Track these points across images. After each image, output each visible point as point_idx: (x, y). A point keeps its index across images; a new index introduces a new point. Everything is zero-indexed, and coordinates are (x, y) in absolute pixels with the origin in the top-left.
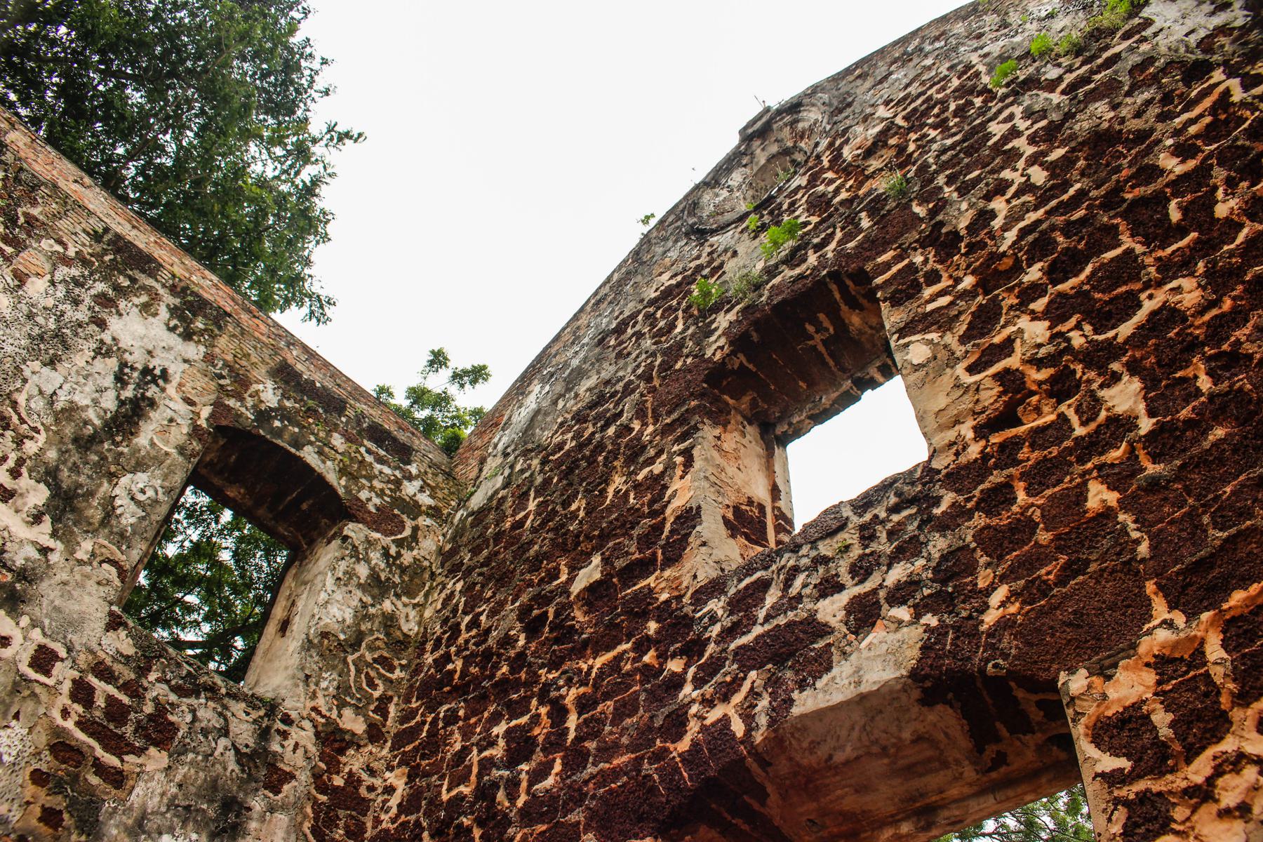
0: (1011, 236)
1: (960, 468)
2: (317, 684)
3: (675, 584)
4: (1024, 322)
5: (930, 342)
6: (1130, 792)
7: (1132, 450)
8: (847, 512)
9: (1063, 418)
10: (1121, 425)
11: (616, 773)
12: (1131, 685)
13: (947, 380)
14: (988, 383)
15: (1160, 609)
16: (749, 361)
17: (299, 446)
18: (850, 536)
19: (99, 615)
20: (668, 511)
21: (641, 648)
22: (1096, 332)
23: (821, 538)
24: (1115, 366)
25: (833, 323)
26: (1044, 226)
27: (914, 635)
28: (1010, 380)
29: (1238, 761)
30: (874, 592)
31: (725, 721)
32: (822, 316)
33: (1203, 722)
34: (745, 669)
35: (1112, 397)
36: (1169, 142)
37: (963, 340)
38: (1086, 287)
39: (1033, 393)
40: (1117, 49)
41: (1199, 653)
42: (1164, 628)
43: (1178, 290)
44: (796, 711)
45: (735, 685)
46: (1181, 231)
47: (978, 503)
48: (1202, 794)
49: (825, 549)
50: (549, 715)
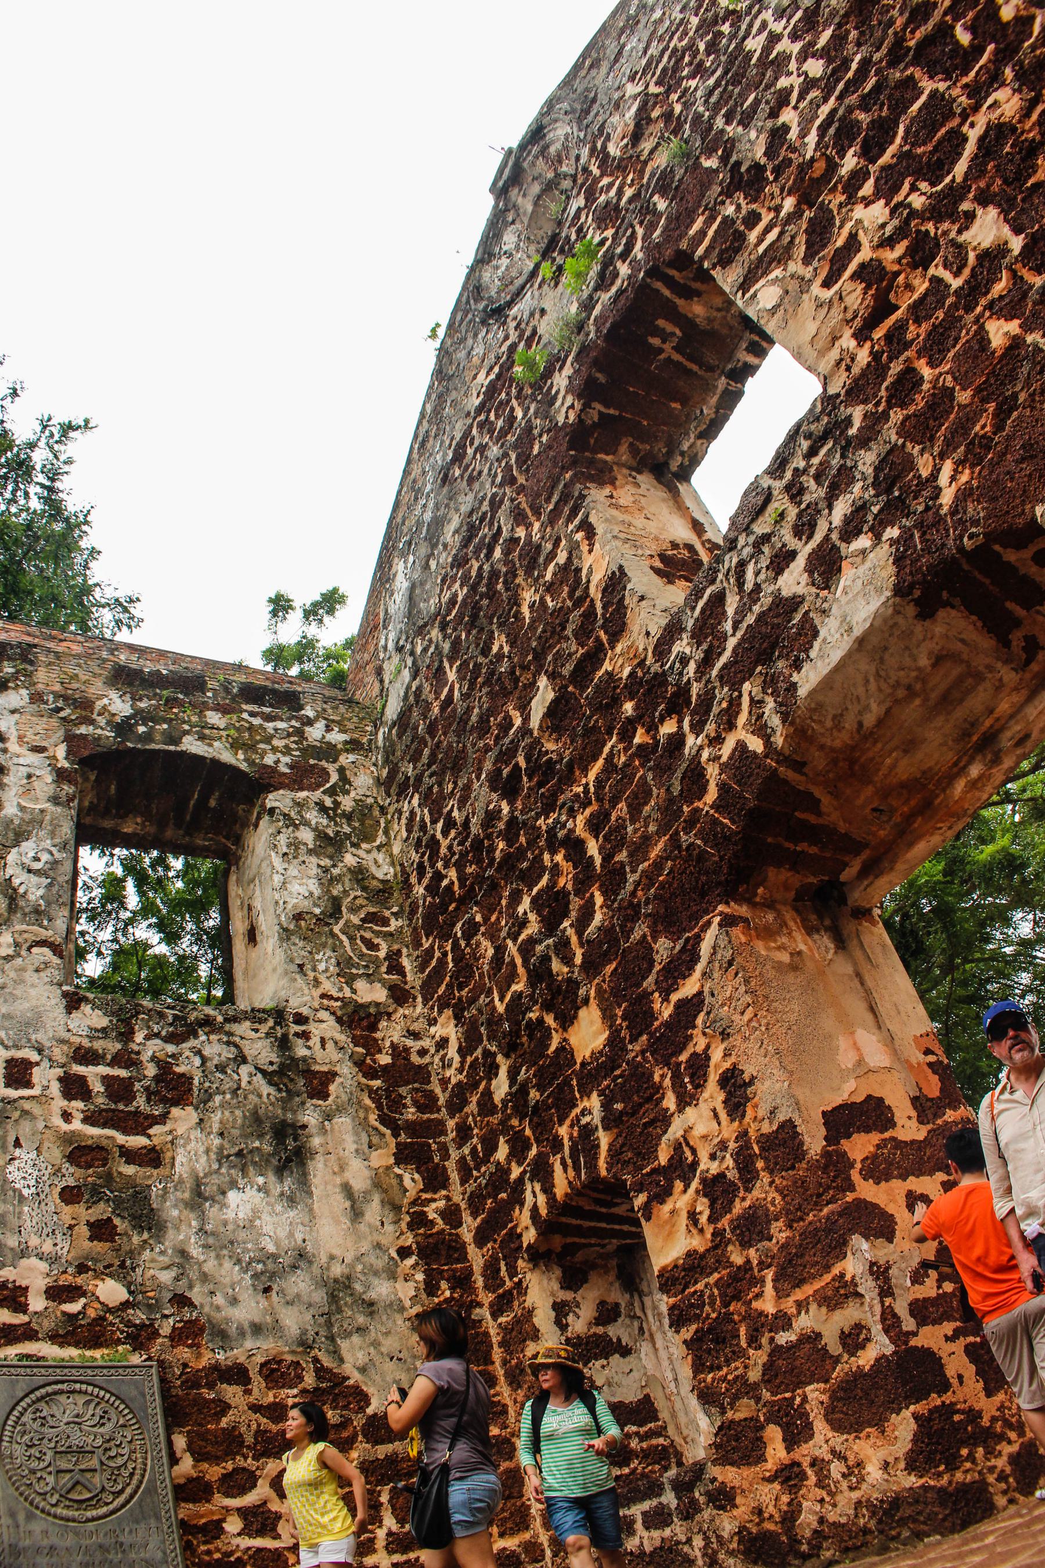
0: (812, 138)
1: (856, 380)
2: (314, 969)
4: (859, 212)
7: (1014, 274)
8: (766, 482)
9: (936, 281)
11: (658, 865)
13: (807, 304)
14: (849, 286)
16: (607, 407)
17: (177, 741)
19: (53, 1002)
21: (626, 736)
22: (933, 184)
23: (753, 520)
24: (965, 206)
25: (676, 324)
26: (840, 112)
27: (883, 554)
28: (871, 275)
30: (827, 538)
31: (741, 746)
32: (661, 323)
34: (736, 686)
35: (974, 237)
38: (907, 148)
39: (897, 274)
44: (802, 692)
45: (734, 705)
47: (888, 402)
50: (567, 858)
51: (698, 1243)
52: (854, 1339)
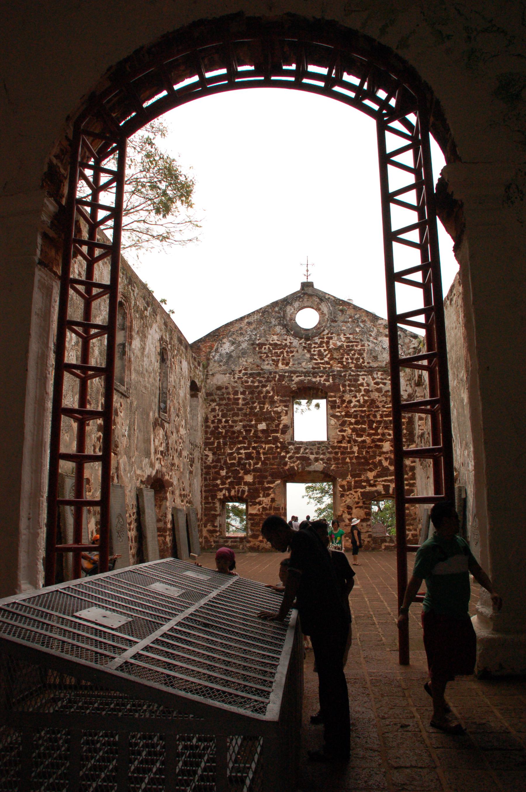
0: (353, 410)
3: (284, 439)
9: (347, 447)
10: (353, 452)
11: (274, 469)
12: (345, 483)
15: (349, 477)
18: (316, 447)
20: (282, 422)
26: (358, 413)
29: (352, 494)
31: (293, 466)
33: (349, 489)
34: (298, 460)
36: (381, 413)
37: (340, 425)
41: (351, 483)
42: (349, 478)
45: (296, 462)
46: (373, 429)
48: (348, 495)
49: (311, 447)
51: (258, 512)
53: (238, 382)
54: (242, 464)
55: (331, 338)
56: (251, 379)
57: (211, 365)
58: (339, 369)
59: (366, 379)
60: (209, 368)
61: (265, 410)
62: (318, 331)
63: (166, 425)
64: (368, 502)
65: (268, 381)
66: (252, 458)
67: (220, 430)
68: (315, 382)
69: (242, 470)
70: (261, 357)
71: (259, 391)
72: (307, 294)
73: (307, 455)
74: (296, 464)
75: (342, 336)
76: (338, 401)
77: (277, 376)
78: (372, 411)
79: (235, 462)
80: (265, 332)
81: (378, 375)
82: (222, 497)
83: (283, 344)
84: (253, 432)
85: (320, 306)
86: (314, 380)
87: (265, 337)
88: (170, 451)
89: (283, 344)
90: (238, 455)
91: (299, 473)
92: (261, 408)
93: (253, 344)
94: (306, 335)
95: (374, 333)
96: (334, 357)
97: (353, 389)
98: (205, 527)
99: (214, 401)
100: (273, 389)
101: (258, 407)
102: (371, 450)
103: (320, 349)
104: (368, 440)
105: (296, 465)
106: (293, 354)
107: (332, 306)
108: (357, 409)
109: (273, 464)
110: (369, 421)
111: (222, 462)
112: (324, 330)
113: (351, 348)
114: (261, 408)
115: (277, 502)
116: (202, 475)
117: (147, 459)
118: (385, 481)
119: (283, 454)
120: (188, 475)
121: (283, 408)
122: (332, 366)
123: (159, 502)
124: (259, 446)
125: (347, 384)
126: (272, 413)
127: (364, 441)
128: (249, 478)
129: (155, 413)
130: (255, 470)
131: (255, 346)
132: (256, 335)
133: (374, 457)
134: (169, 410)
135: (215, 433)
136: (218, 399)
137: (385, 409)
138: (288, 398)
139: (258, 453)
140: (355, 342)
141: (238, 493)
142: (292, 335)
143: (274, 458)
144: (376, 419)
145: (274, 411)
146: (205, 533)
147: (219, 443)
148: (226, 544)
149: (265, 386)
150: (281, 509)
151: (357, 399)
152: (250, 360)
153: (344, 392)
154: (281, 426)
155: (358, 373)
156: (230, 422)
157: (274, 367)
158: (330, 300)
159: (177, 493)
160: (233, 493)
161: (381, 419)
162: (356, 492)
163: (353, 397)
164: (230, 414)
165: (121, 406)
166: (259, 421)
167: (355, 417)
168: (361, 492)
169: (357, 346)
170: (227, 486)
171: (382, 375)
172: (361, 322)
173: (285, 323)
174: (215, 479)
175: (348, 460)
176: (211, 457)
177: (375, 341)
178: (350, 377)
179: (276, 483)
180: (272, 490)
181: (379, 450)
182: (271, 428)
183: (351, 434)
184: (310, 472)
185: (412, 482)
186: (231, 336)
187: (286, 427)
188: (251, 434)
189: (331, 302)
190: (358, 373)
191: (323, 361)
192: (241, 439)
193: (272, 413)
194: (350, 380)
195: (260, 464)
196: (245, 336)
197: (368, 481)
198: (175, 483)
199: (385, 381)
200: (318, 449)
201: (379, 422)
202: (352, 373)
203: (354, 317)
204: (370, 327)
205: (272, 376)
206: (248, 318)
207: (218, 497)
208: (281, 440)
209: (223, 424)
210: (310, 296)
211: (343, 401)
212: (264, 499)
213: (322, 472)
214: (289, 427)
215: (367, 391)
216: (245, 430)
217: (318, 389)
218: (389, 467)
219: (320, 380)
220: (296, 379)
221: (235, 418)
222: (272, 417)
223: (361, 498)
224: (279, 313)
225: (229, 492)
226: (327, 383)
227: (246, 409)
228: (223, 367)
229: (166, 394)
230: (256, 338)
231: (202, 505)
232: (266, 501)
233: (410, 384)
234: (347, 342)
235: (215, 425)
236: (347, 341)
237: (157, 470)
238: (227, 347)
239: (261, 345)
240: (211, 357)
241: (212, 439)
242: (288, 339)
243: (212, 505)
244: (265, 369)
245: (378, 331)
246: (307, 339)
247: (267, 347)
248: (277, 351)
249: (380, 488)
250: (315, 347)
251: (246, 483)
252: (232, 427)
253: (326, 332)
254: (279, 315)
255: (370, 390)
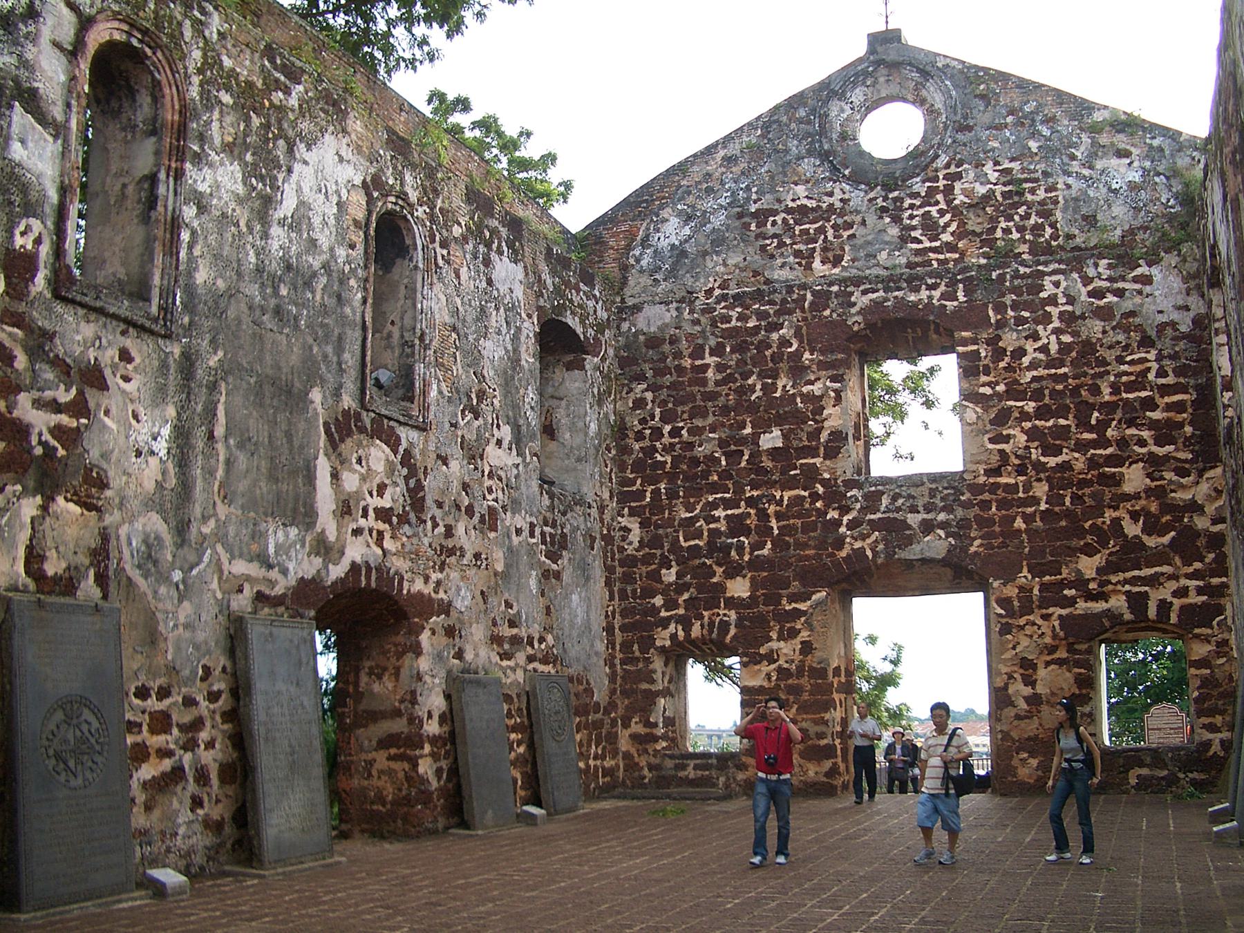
0: (1029, 375)
3: (832, 471)
5: (976, 413)
6: (1004, 621)
8: (925, 480)
10: (1035, 501)
11: (808, 558)
12: (1011, 591)
15: (1025, 572)
20: (826, 424)
24: (1042, 475)
26: (1044, 383)
29: (1034, 624)
33: (1027, 609)
36: (1112, 378)
37: (991, 422)
40: (1127, 285)
43: (1077, 459)
45: (869, 536)
46: (1091, 429)
48: (1022, 628)
49: (912, 491)
51: (766, 684)
52: (821, 736)
53: (703, 320)
54: (720, 550)
55: (959, 176)
56: (739, 310)
57: (631, 282)
58: (983, 261)
59: (1064, 284)
60: (627, 292)
61: (777, 395)
62: (918, 160)
63: (407, 435)
64: (1084, 647)
65: (784, 311)
66: (747, 532)
67: (659, 458)
68: (915, 305)
69: (720, 565)
70: (763, 248)
71: (761, 342)
72: (889, 64)
73: (898, 516)
74: (869, 541)
75: (988, 168)
76: (983, 354)
77: (809, 296)
78: (1085, 374)
79: (701, 544)
80: (772, 178)
81: (1100, 270)
82: (668, 643)
83: (824, 205)
84: (746, 457)
85: (924, 93)
86: (912, 298)
87: (773, 190)
88: (432, 510)
89: (824, 205)
90: (708, 524)
91: (878, 567)
92: (768, 389)
93: (740, 216)
94: (887, 178)
95: (1082, 148)
96: (970, 227)
97: (1026, 314)
98: (626, 725)
99: (641, 377)
100: (798, 334)
101: (758, 387)
102: (1087, 491)
103: (927, 209)
104: (1079, 462)
105: (869, 544)
106: (851, 232)
107: (956, 86)
108: (1042, 372)
109: (805, 546)
110: (1077, 405)
111: (667, 546)
112: (937, 156)
113: (1016, 199)
114: (768, 389)
115: (818, 654)
116: (608, 583)
117: (293, 532)
118: (1133, 581)
119: (833, 514)
120: (533, 584)
121: (828, 383)
122: (963, 254)
123: (393, 660)
124: (763, 496)
125: (1008, 303)
126: (799, 400)
127: (1066, 466)
128: (739, 588)
129: (337, 394)
130: (755, 564)
131: (747, 219)
132: (748, 189)
133: (1098, 511)
134: (424, 393)
135: (647, 468)
136: (649, 374)
137: (1125, 368)
138: (840, 356)
139: (763, 515)
140: (1026, 180)
141: (711, 632)
142: (848, 179)
143: (806, 528)
144: (1098, 399)
145: (802, 395)
146: (624, 744)
147: (657, 492)
148: (682, 774)
149: (777, 327)
150: (830, 674)
151: (1040, 344)
152: (735, 259)
153: (1001, 325)
154: (824, 436)
155: (1040, 268)
156: (684, 432)
157: (799, 271)
158: (948, 71)
159: (478, 632)
160: (696, 631)
161: (1114, 398)
162: (1046, 617)
163: (1026, 338)
164: (683, 412)
165: (125, 356)
166: (763, 426)
167: (1037, 395)
168: (1060, 616)
169: (1033, 191)
170: (681, 611)
171: (1110, 267)
172: (1042, 122)
173: (826, 147)
174: (649, 593)
175: (1019, 523)
176: (636, 535)
177: (1086, 172)
178: (1016, 283)
179: (814, 597)
180: (803, 619)
181: (1113, 489)
182: (795, 443)
183: (1027, 448)
184: (909, 564)
185: (1215, 581)
186: (682, 199)
187: (838, 437)
188: (743, 464)
189: (951, 78)
190: (1040, 268)
191: (937, 244)
192: (716, 478)
193: (799, 400)
194: (1014, 290)
195: (769, 545)
196: (719, 194)
197: (1080, 582)
198: (463, 601)
199: (1120, 285)
200: (932, 496)
201: (1109, 408)
202: (1022, 270)
203: (1021, 109)
204: (1071, 134)
205: (795, 296)
206: (725, 147)
207: (658, 643)
208: (826, 476)
209: (666, 440)
210: (894, 66)
211: (999, 353)
212: (782, 644)
213: (944, 562)
214: (846, 438)
215: (1069, 319)
216: (724, 454)
217: (923, 324)
218: (1145, 538)
219: (930, 298)
220: (861, 300)
221: (699, 422)
222: (798, 410)
223: (1062, 634)
224: (809, 122)
225: (687, 630)
226: (950, 305)
227: (727, 395)
228: (663, 285)
229: (413, 346)
230: (748, 199)
231: (612, 666)
232: (787, 650)
233: (1199, 287)
234: (1004, 185)
235: (647, 443)
236: (1003, 180)
237: (353, 564)
238: (672, 231)
239: (762, 216)
240: (632, 261)
241: (639, 482)
242: (837, 191)
243: (641, 665)
244: (777, 281)
245: (1094, 143)
246: (888, 188)
247: (779, 219)
248: (807, 226)
249: (1118, 603)
250: (912, 207)
251: (732, 603)
252: (690, 446)
253: (943, 159)
254: (809, 128)
255: (1078, 313)
